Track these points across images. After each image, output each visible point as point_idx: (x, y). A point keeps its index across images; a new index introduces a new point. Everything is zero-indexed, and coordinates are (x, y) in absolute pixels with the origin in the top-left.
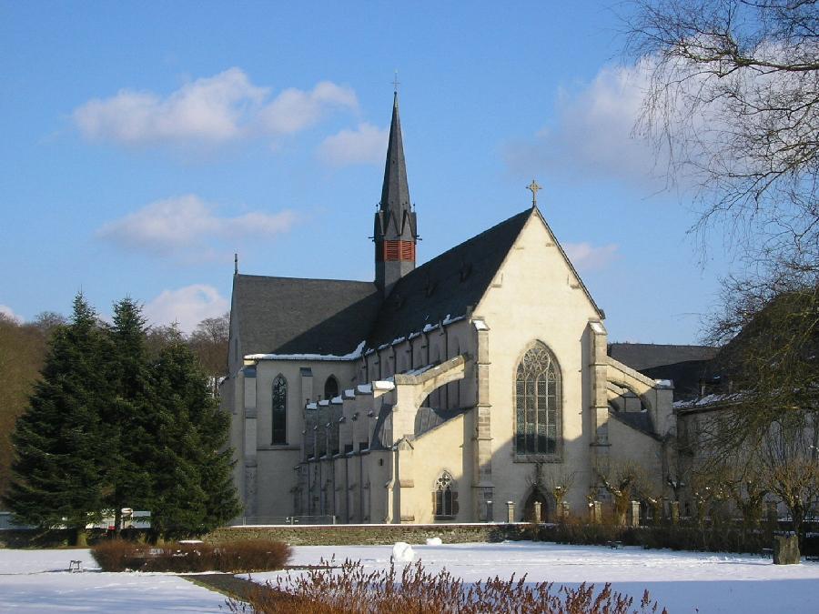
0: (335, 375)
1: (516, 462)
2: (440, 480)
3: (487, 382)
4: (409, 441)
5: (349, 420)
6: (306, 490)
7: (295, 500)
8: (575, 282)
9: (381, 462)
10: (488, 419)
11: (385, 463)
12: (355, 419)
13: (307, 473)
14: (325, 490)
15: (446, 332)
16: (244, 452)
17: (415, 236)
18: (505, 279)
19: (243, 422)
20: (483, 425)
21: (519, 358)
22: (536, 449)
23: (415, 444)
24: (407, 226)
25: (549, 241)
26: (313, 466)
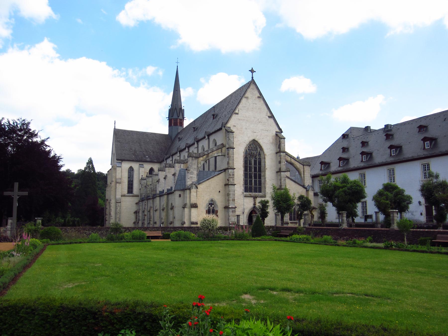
0: (153, 167)
1: (246, 196)
2: (209, 204)
3: (233, 157)
4: (196, 185)
5: (162, 180)
6: (141, 212)
7: (136, 216)
8: (270, 115)
9: (180, 196)
10: (234, 174)
11: (182, 196)
12: (165, 178)
13: (141, 205)
14: (149, 211)
15: (209, 138)
16: (116, 197)
17: (184, 118)
18: (240, 111)
19: (116, 185)
20: (231, 178)
21: (246, 147)
22: (253, 191)
23: (199, 186)
24: (181, 114)
25: (259, 96)
26: (144, 202)
